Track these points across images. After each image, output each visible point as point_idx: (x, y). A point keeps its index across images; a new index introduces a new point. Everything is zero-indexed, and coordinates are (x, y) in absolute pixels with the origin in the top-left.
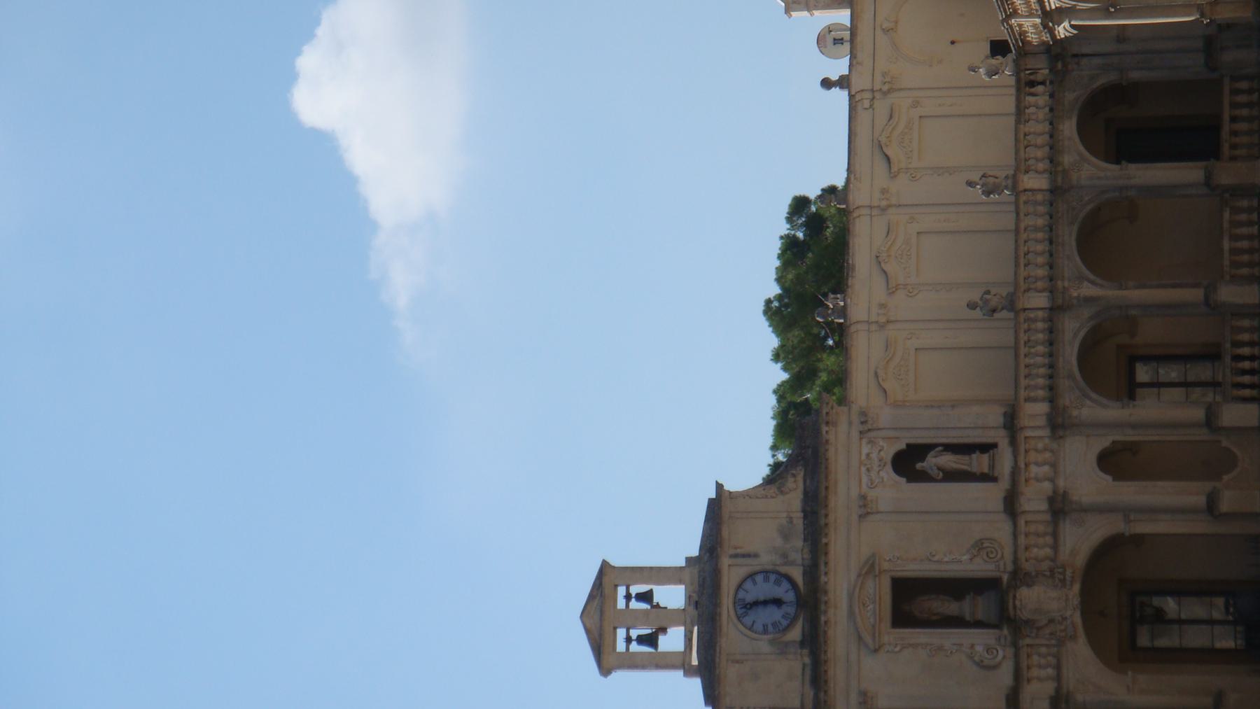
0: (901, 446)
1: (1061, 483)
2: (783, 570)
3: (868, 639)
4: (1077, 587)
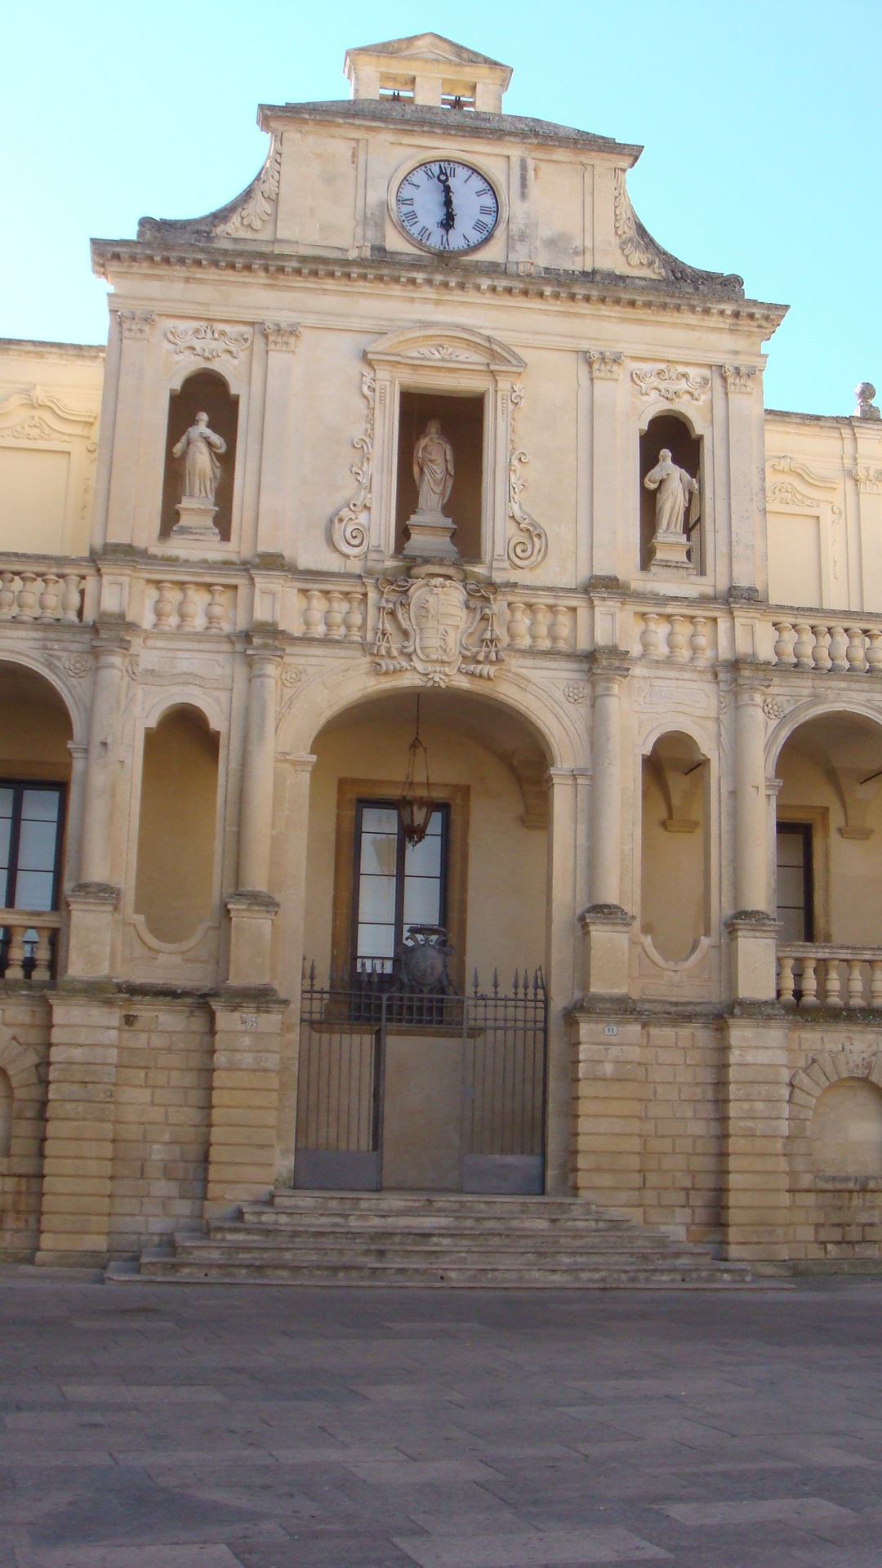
0: (699, 427)
1: (638, 671)
2: (500, 232)
3: (382, 345)
4: (463, 683)
